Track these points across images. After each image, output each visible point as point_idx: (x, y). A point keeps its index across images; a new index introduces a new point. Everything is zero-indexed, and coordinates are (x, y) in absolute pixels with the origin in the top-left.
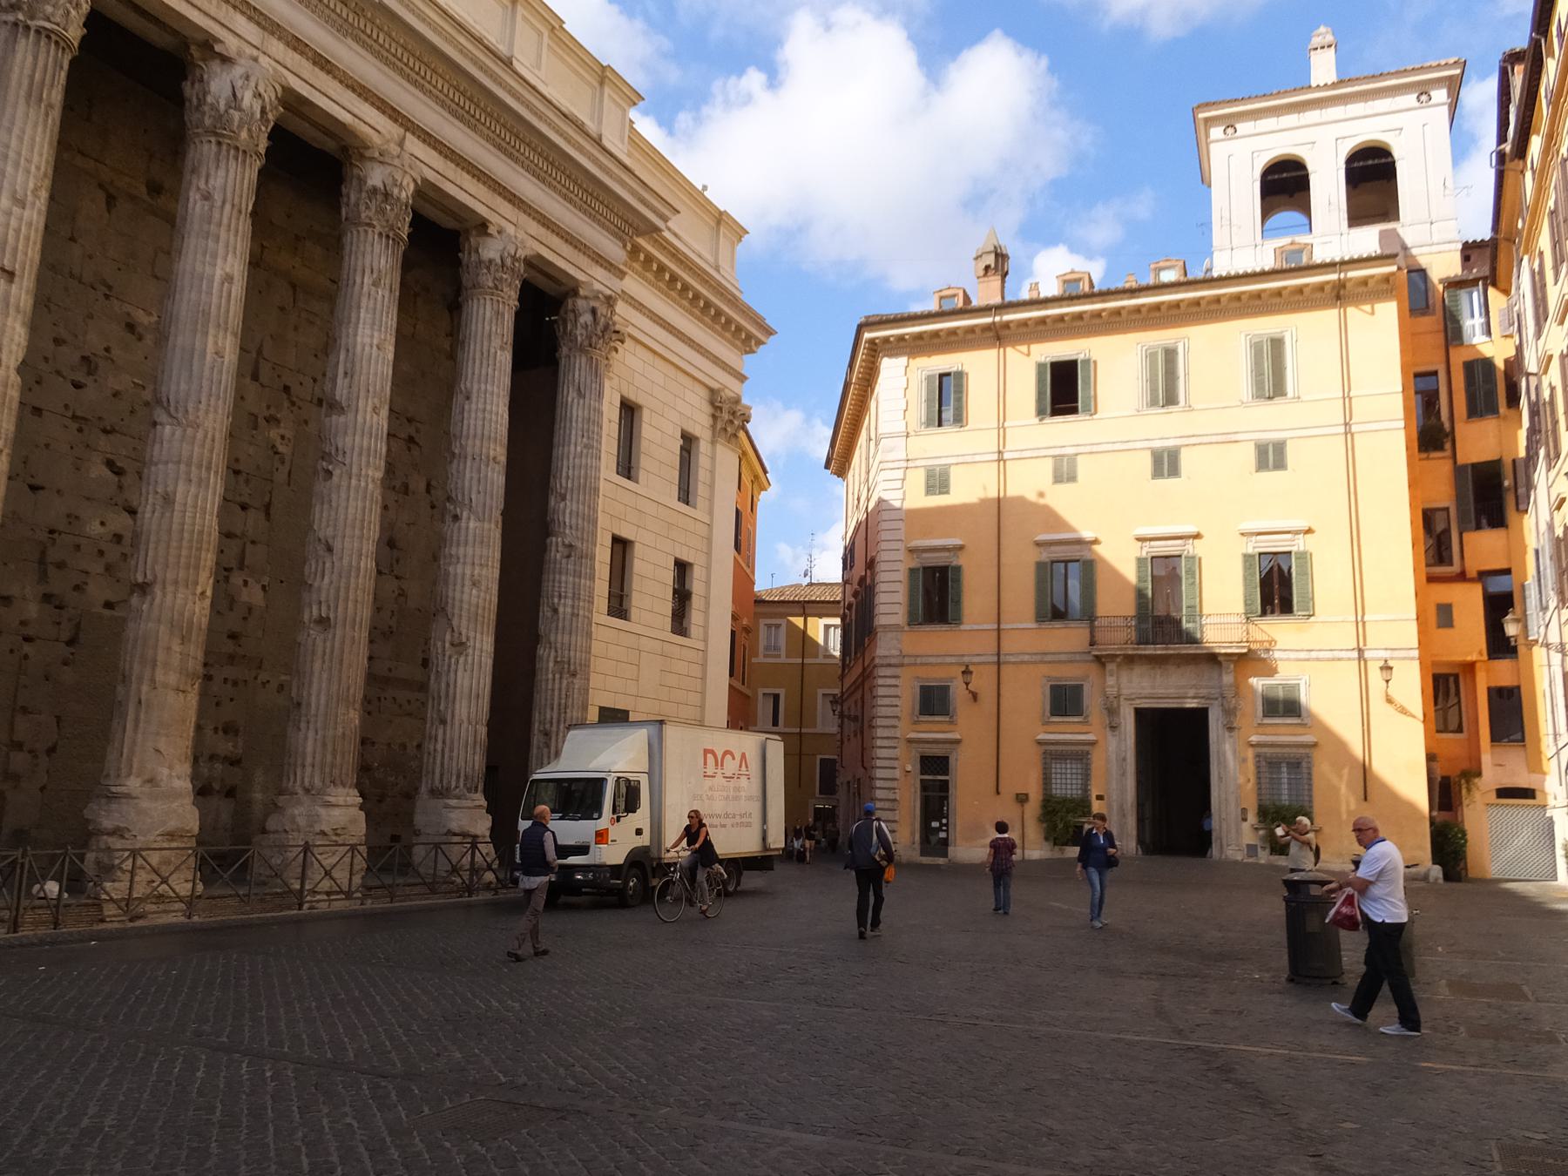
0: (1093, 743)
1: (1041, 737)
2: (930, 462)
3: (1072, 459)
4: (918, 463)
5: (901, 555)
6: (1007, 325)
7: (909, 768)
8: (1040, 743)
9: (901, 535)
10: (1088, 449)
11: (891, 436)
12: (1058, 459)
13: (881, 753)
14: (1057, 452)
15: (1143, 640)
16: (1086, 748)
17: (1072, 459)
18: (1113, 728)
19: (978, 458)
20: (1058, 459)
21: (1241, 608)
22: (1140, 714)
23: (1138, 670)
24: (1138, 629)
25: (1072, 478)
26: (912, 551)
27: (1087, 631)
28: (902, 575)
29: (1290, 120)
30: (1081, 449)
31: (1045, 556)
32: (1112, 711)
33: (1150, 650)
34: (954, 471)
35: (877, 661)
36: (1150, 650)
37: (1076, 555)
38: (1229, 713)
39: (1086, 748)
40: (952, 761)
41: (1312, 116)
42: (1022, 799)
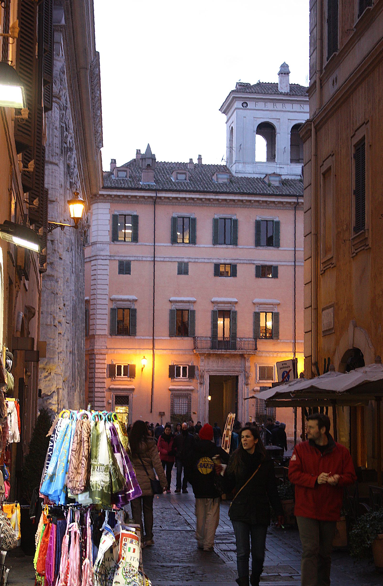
0: (192, 390)
1: (170, 387)
2: (121, 258)
3: (187, 264)
4: (116, 258)
5: (107, 302)
6: (160, 198)
7: (110, 401)
8: (170, 390)
9: (107, 292)
10: (193, 260)
11: (102, 243)
12: (180, 264)
13: (97, 394)
14: (180, 260)
15: (213, 348)
16: (189, 392)
17: (187, 264)
18: (201, 384)
19: (144, 259)
20: (180, 264)
21: (251, 335)
22: (211, 378)
23: (211, 359)
24: (212, 342)
25: (186, 273)
26: (112, 300)
27: (192, 342)
28: (107, 311)
29: (270, 106)
30: (191, 260)
31: (174, 307)
32: (202, 377)
33: (219, 352)
34: (132, 263)
35: (95, 351)
36: (219, 352)
37: (187, 308)
38: (247, 378)
39: (189, 392)
40: (130, 398)
41: (279, 106)
42: (162, 414)
